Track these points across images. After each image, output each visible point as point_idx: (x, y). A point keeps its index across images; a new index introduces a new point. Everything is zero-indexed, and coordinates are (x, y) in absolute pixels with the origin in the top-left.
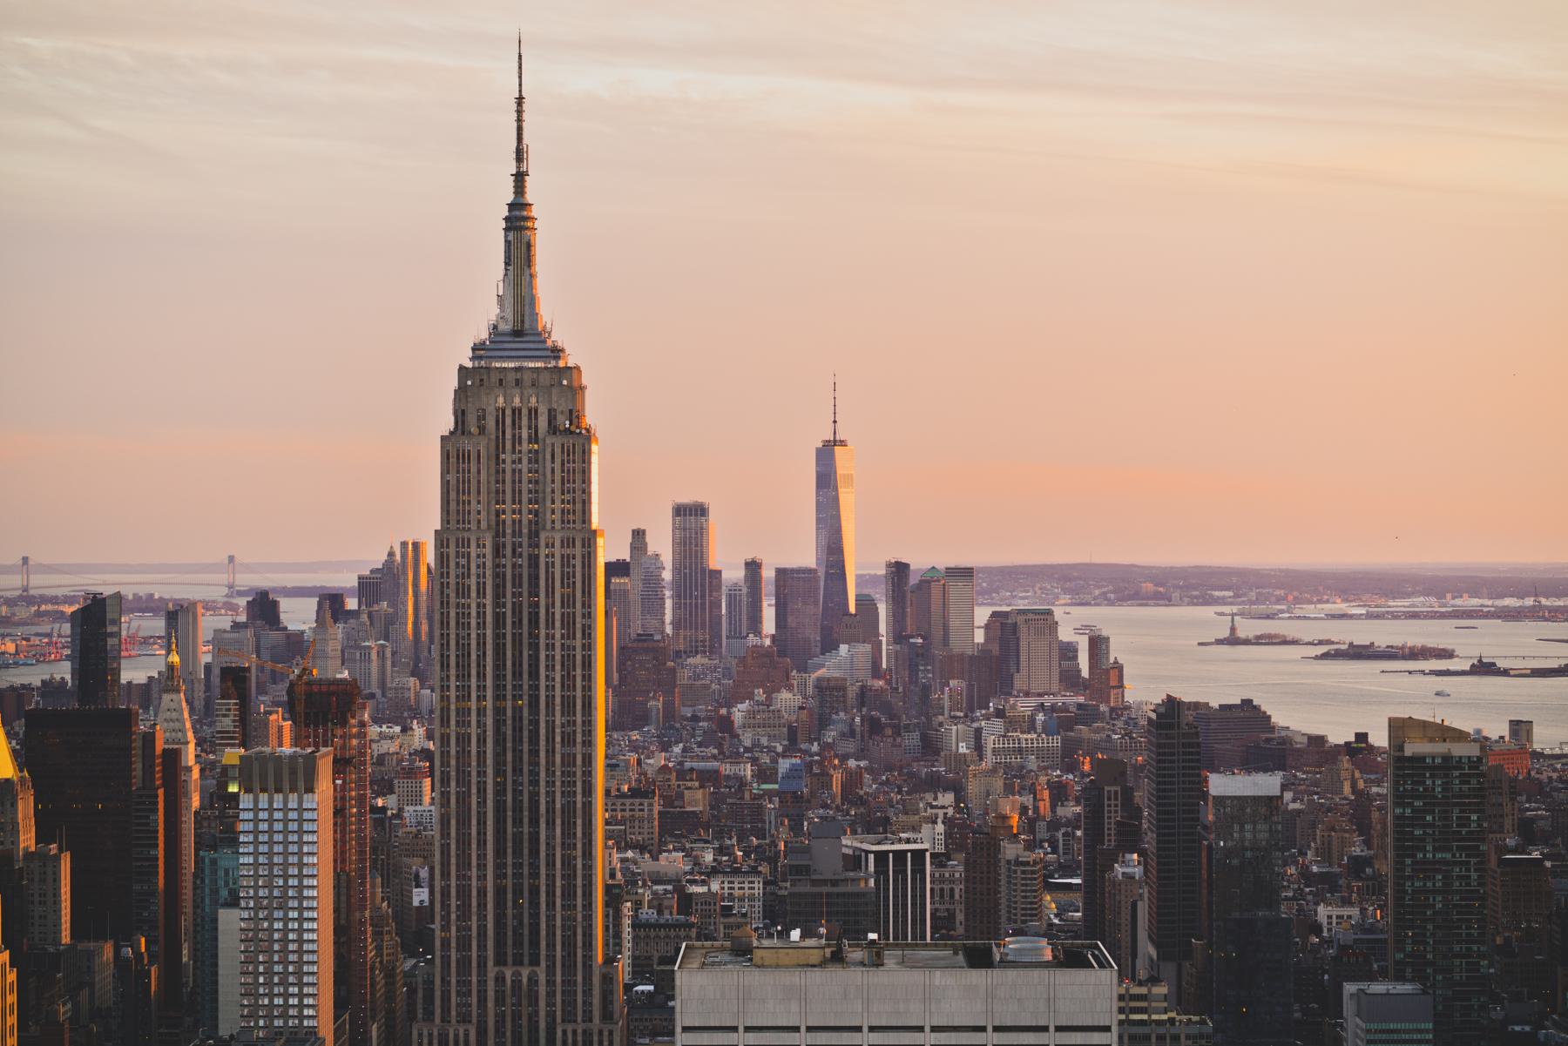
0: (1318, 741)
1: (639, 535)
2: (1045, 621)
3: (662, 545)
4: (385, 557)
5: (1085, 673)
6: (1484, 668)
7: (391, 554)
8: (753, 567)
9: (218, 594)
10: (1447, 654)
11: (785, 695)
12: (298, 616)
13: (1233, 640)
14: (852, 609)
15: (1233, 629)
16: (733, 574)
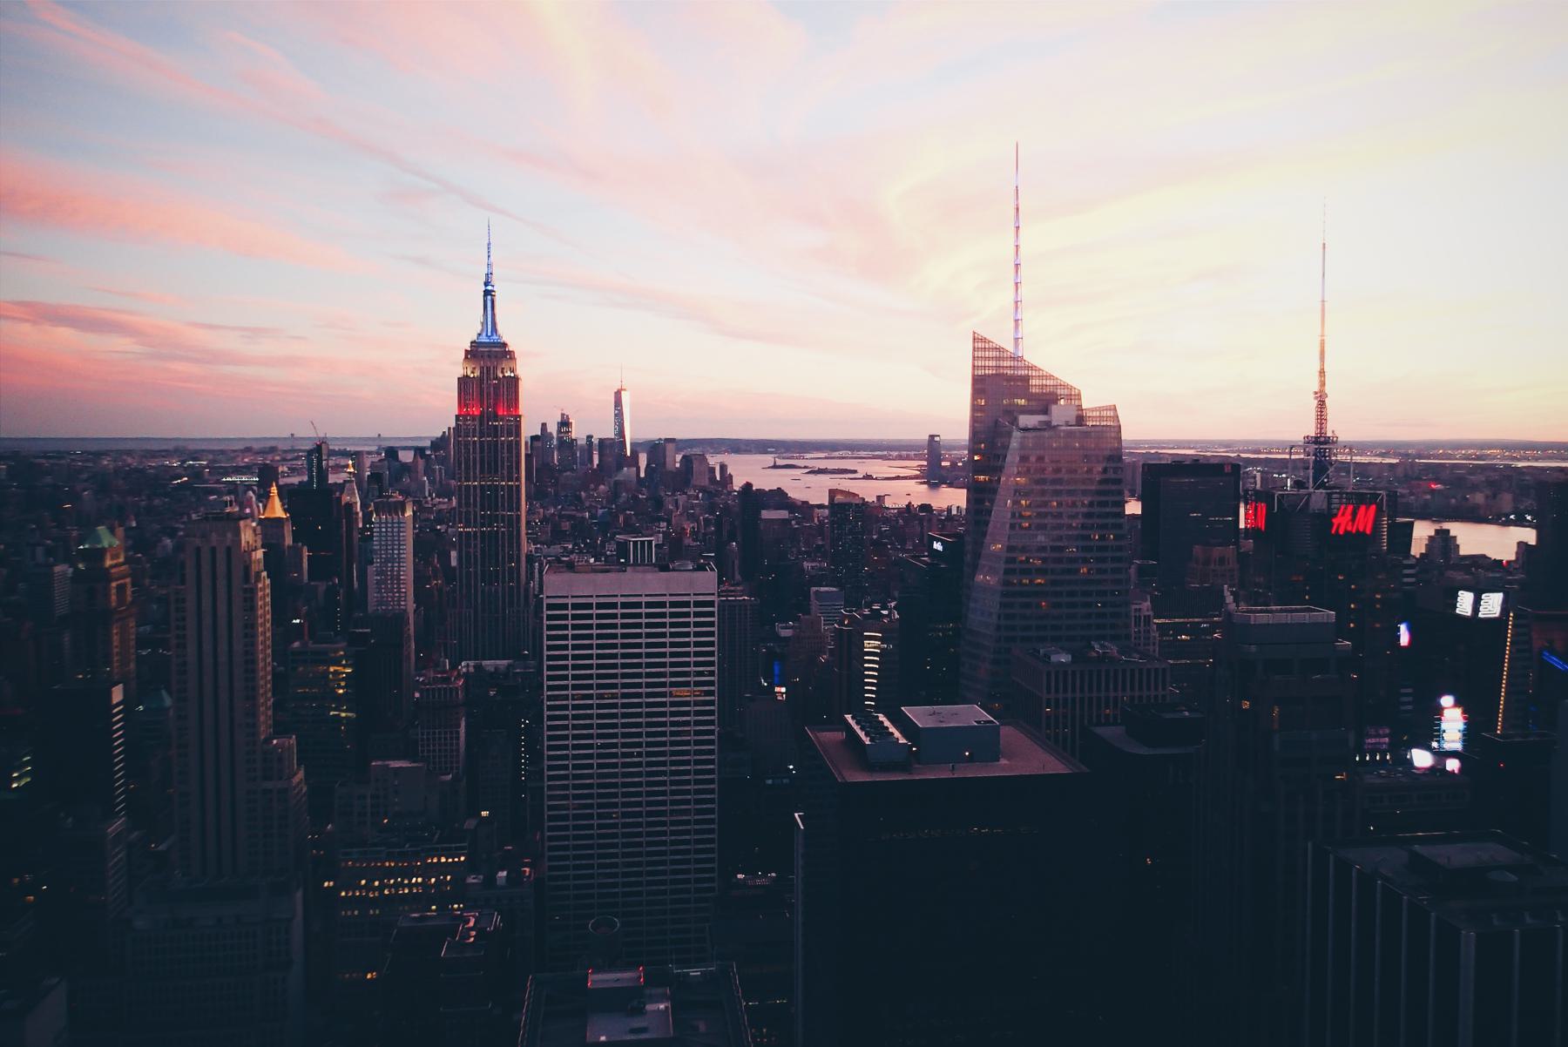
0: (806, 503)
1: (544, 425)
2: (703, 458)
3: (553, 429)
4: (439, 434)
5: (718, 478)
6: (868, 477)
7: (444, 432)
8: (589, 437)
9: (374, 448)
10: (855, 472)
11: (602, 487)
12: (406, 457)
13: (775, 467)
14: (629, 454)
15: (775, 463)
16: (582, 442)
